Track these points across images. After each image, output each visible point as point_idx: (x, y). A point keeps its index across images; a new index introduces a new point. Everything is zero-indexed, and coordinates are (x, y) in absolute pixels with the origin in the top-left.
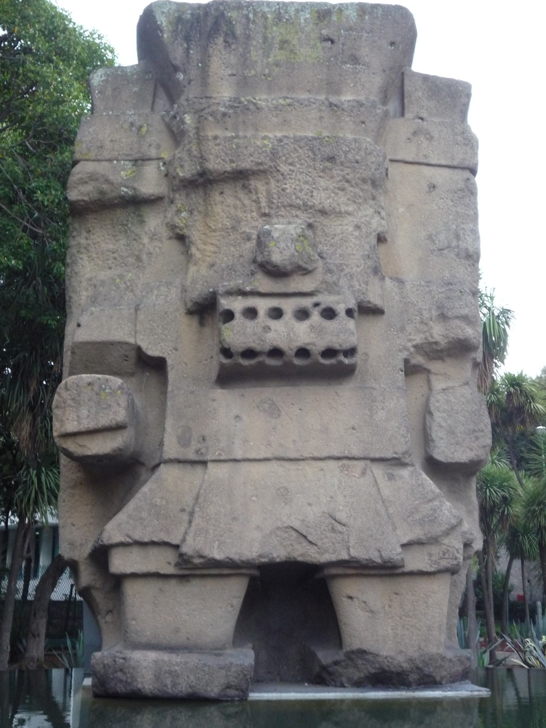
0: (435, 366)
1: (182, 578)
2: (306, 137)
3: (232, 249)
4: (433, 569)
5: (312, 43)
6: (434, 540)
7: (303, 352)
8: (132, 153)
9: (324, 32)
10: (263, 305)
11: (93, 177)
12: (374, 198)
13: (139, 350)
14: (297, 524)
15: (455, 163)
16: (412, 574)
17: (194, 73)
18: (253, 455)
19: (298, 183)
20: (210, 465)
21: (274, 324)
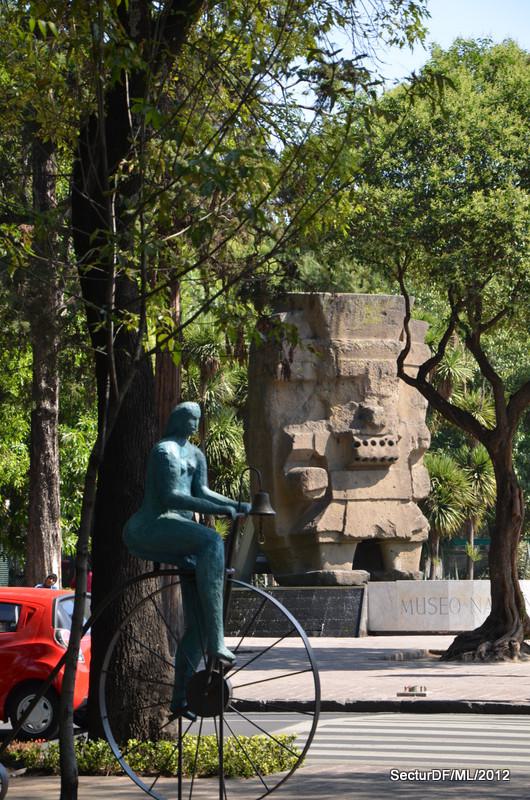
1: (339, 544)
6: (420, 530)
16: (412, 542)
17: (333, 328)
18: (363, 498)
20: (349, 503)
21: (374, 448)
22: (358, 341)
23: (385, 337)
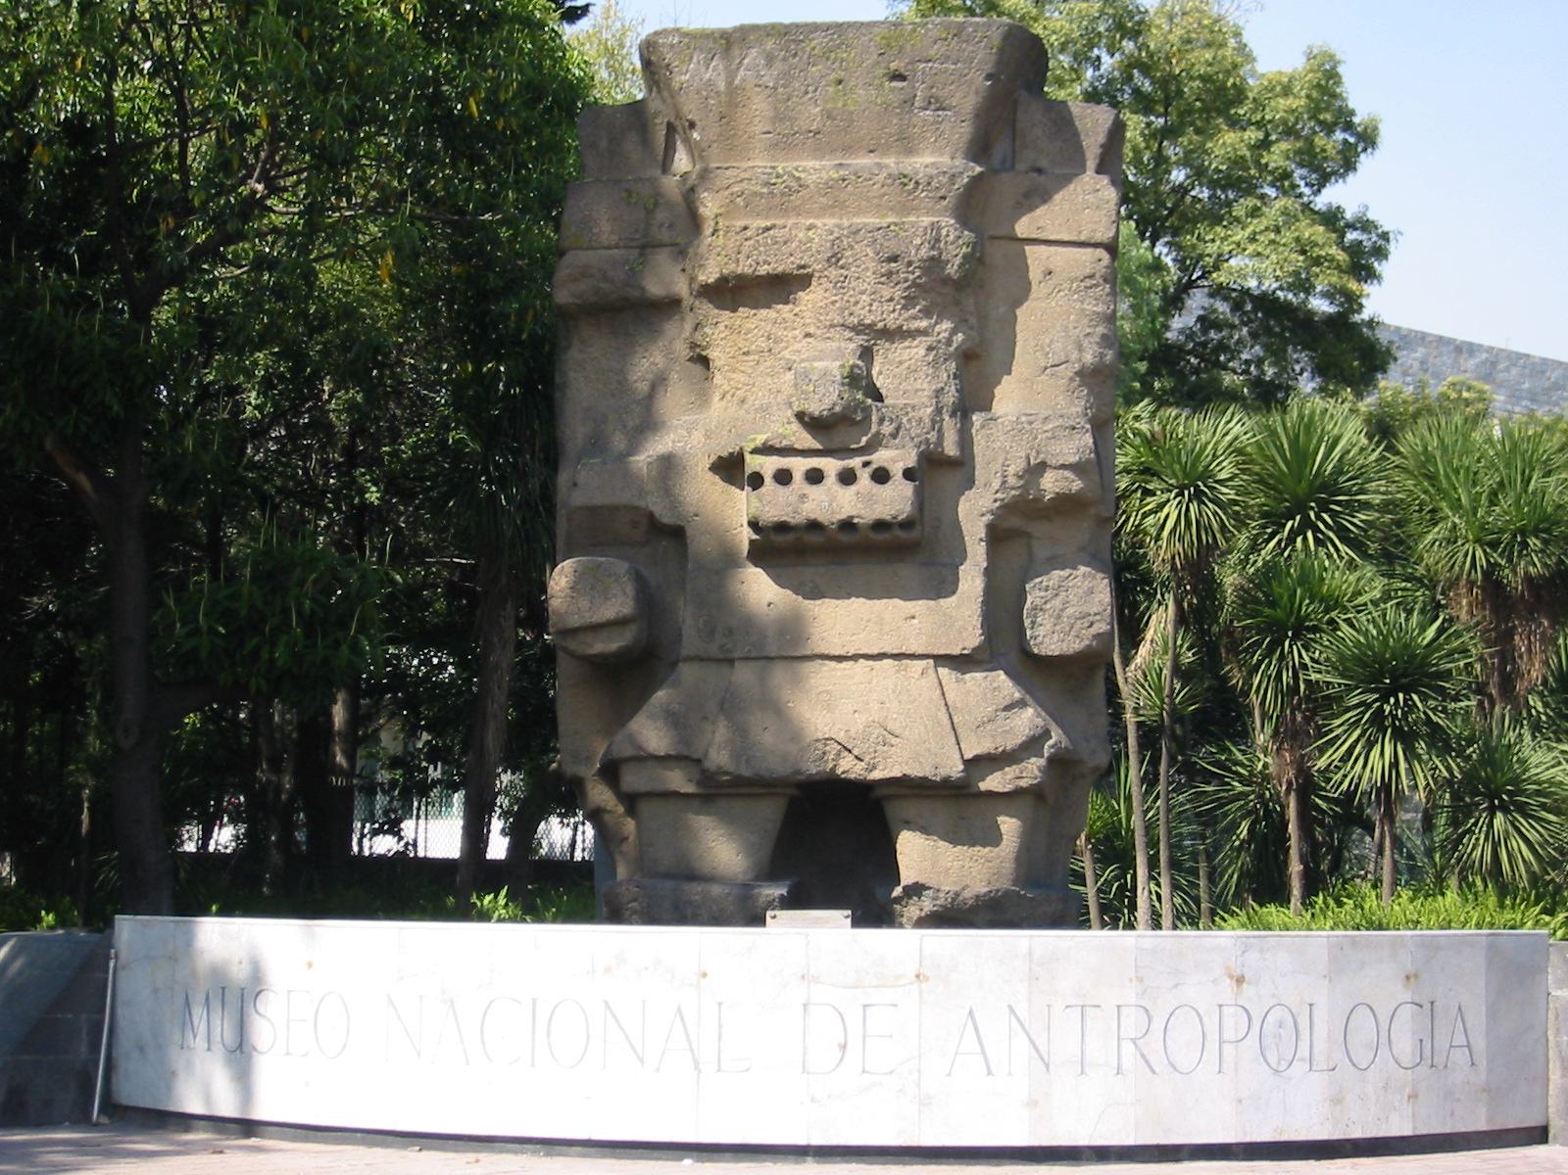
0: (1039, 529)
2: (866, 225)
3: (769, 380)
4: (1006, 790)
5: (877, 82)
7: (847, 525)
8: (637, 236)
9: (893, 66)
10: (799, 465)
11: (585, 273)
12: (957, 303)
13: (651, 515)
14: (841, 737)
15: (1083, 238)
19: (852, 292)
21: (815, 492)
22: (814, 169)
23: (910, 151)
